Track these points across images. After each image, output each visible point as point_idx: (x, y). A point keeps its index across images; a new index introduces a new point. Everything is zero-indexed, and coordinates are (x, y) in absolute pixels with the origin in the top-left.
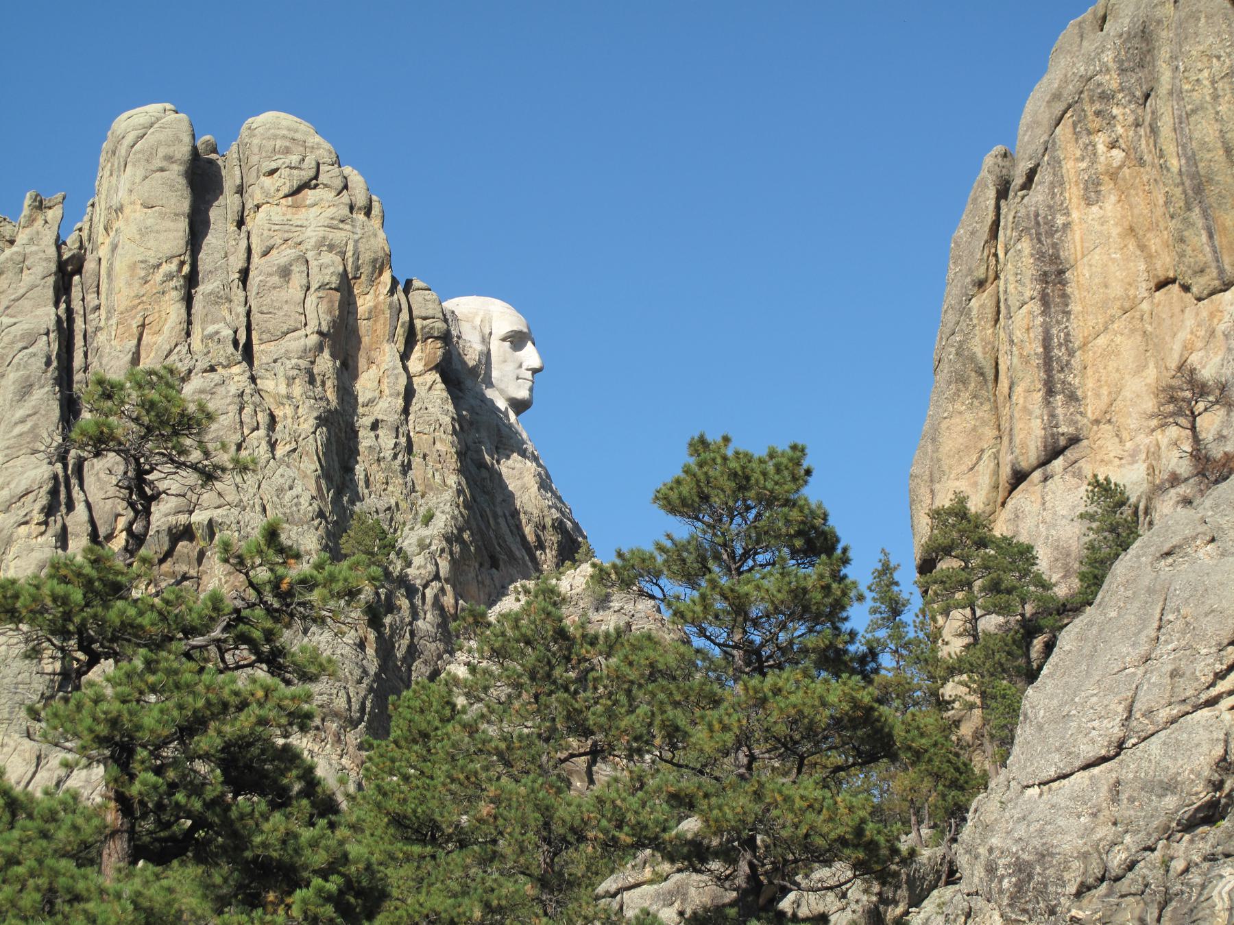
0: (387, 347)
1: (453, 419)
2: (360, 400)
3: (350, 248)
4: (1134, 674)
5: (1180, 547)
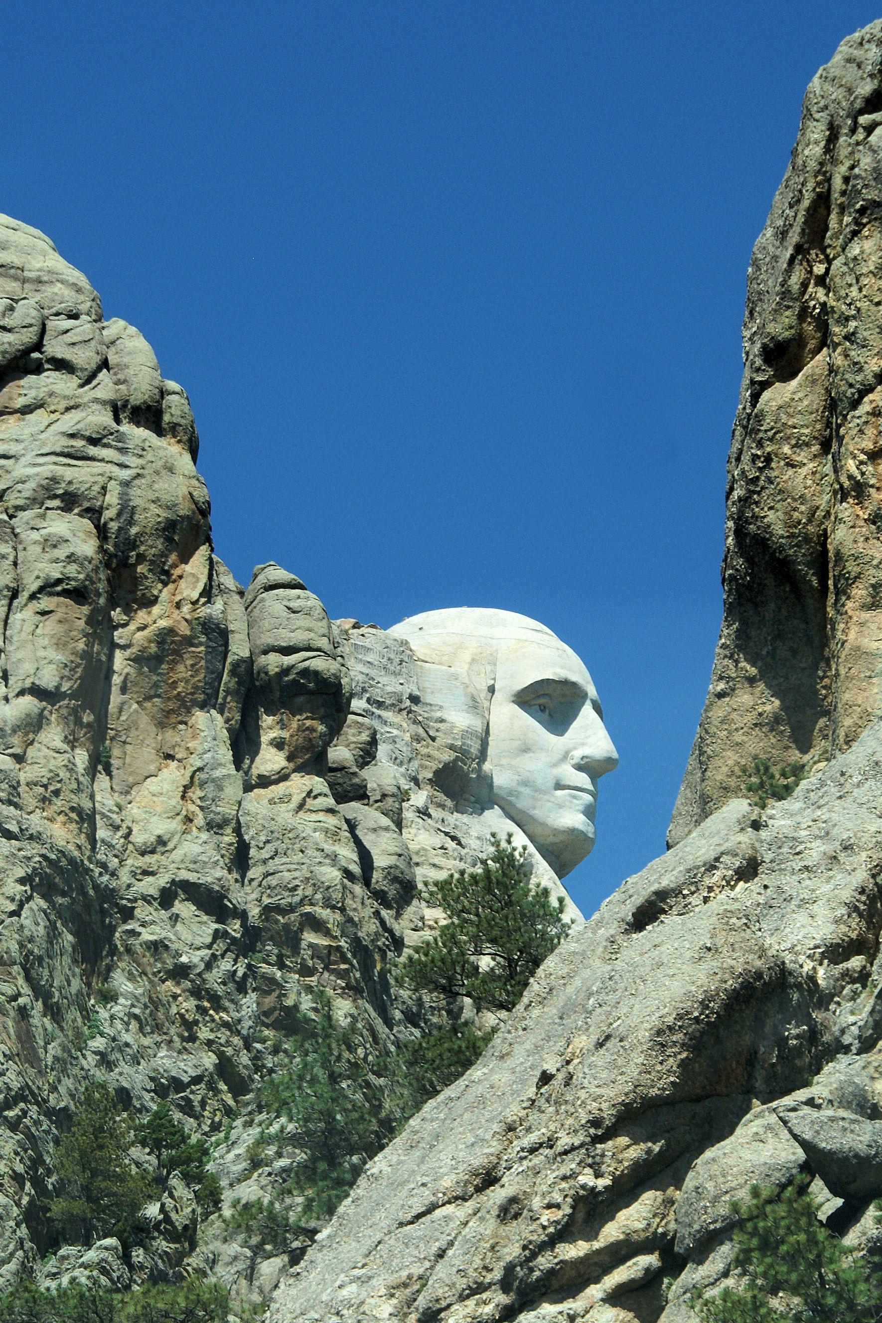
0: (200, 718)
1: (348, 874)
2: (139, 838)
3: (112, 499)
4: (447, 1218)
5: (676, 892)
